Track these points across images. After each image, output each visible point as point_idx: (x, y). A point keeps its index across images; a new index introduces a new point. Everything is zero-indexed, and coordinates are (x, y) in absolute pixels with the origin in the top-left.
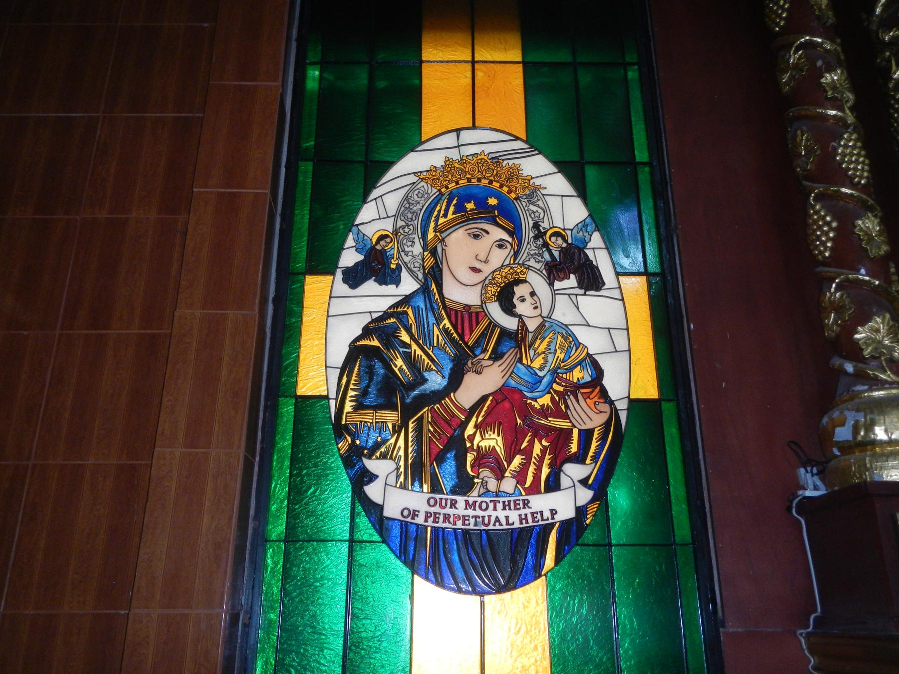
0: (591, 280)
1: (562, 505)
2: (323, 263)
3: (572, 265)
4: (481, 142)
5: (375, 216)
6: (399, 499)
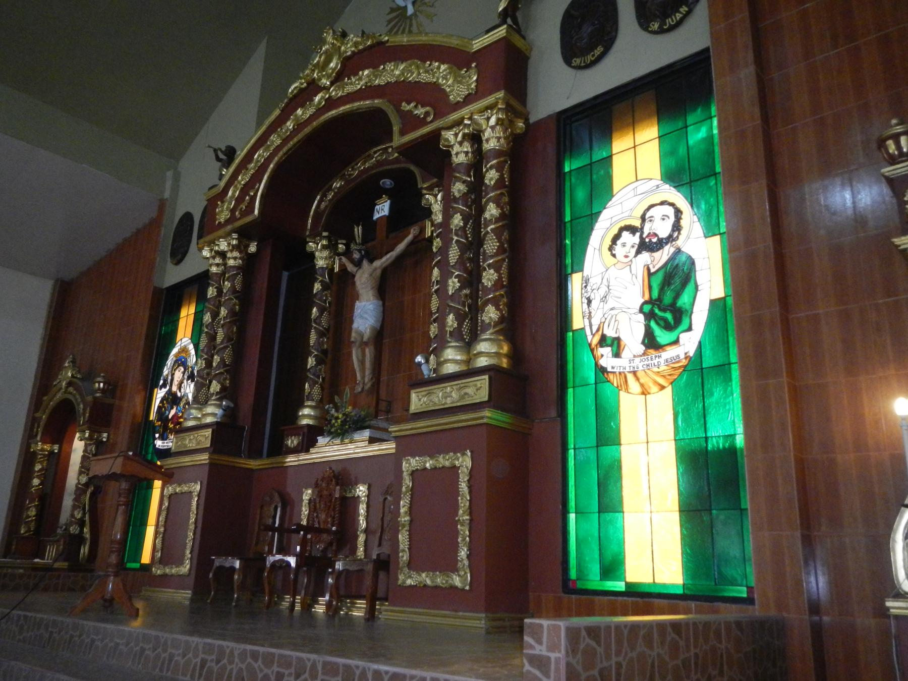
2: (157, 386)
5: (166, 371)
6: (159, 443)
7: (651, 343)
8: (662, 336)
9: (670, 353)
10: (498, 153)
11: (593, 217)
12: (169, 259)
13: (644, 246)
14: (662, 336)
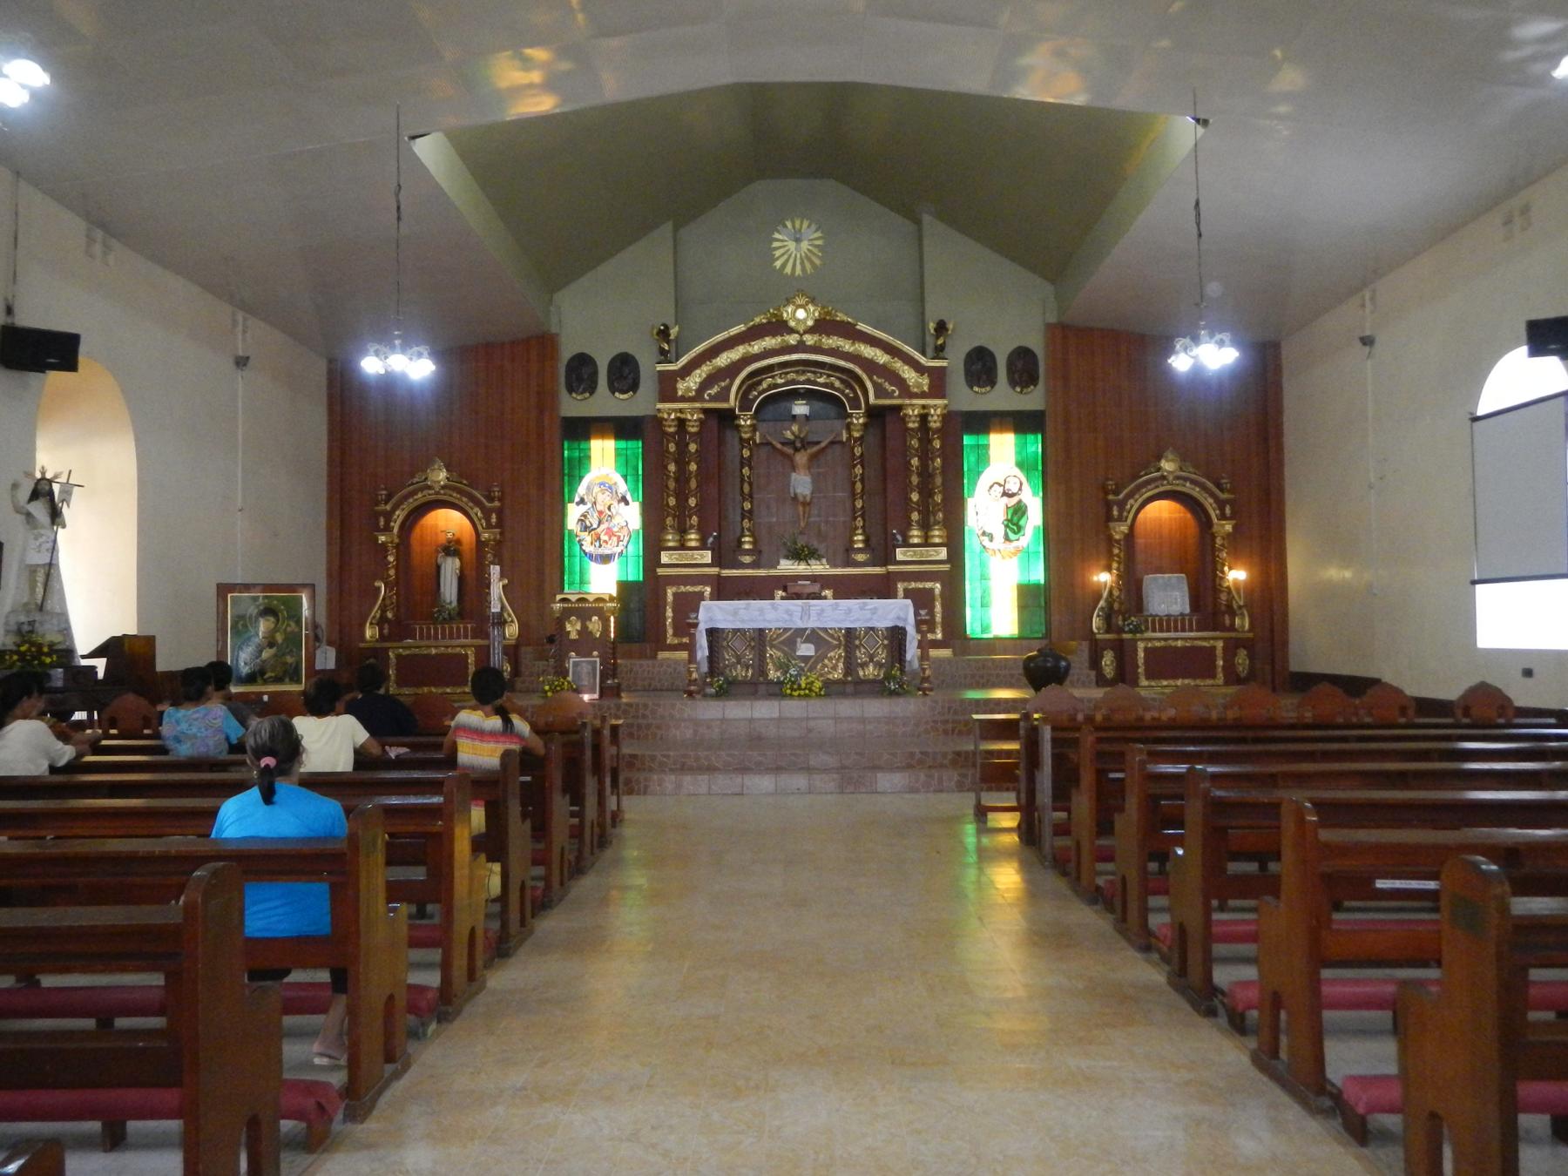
0: (627, 503)
1: (618, 550)
2: (571, 501)
3: (624, 500)
4: (604, 471)
5: (581, 490)
6: (588, 548)
7: (1007, 538)
8: (1011, 536)
9: (1015, 544)
10: (937, 431)
11: (979, 474)
12: (563, 391)
13: (1005, 494)
14: (1011, 536)
